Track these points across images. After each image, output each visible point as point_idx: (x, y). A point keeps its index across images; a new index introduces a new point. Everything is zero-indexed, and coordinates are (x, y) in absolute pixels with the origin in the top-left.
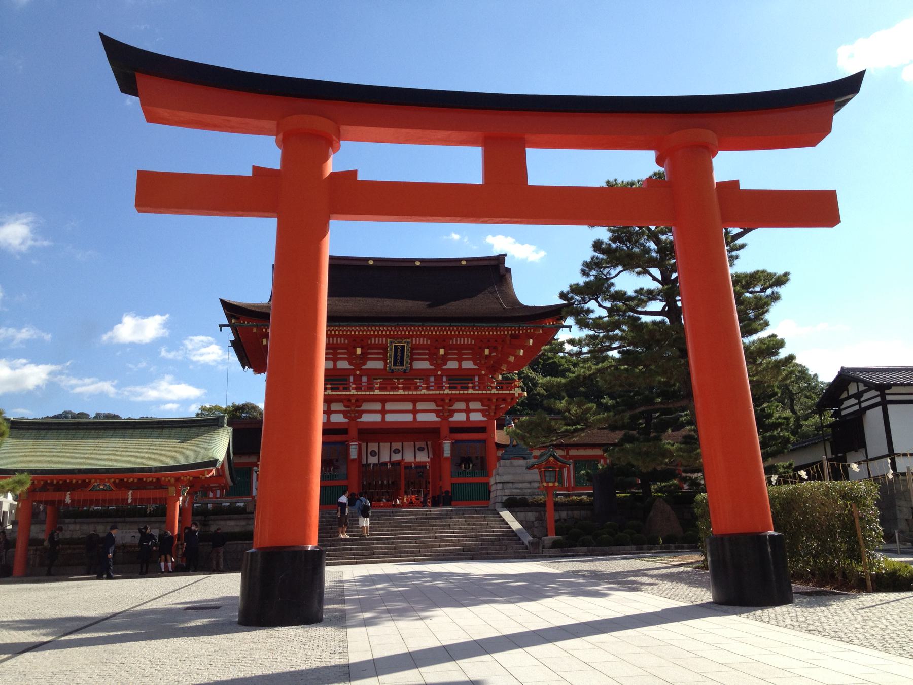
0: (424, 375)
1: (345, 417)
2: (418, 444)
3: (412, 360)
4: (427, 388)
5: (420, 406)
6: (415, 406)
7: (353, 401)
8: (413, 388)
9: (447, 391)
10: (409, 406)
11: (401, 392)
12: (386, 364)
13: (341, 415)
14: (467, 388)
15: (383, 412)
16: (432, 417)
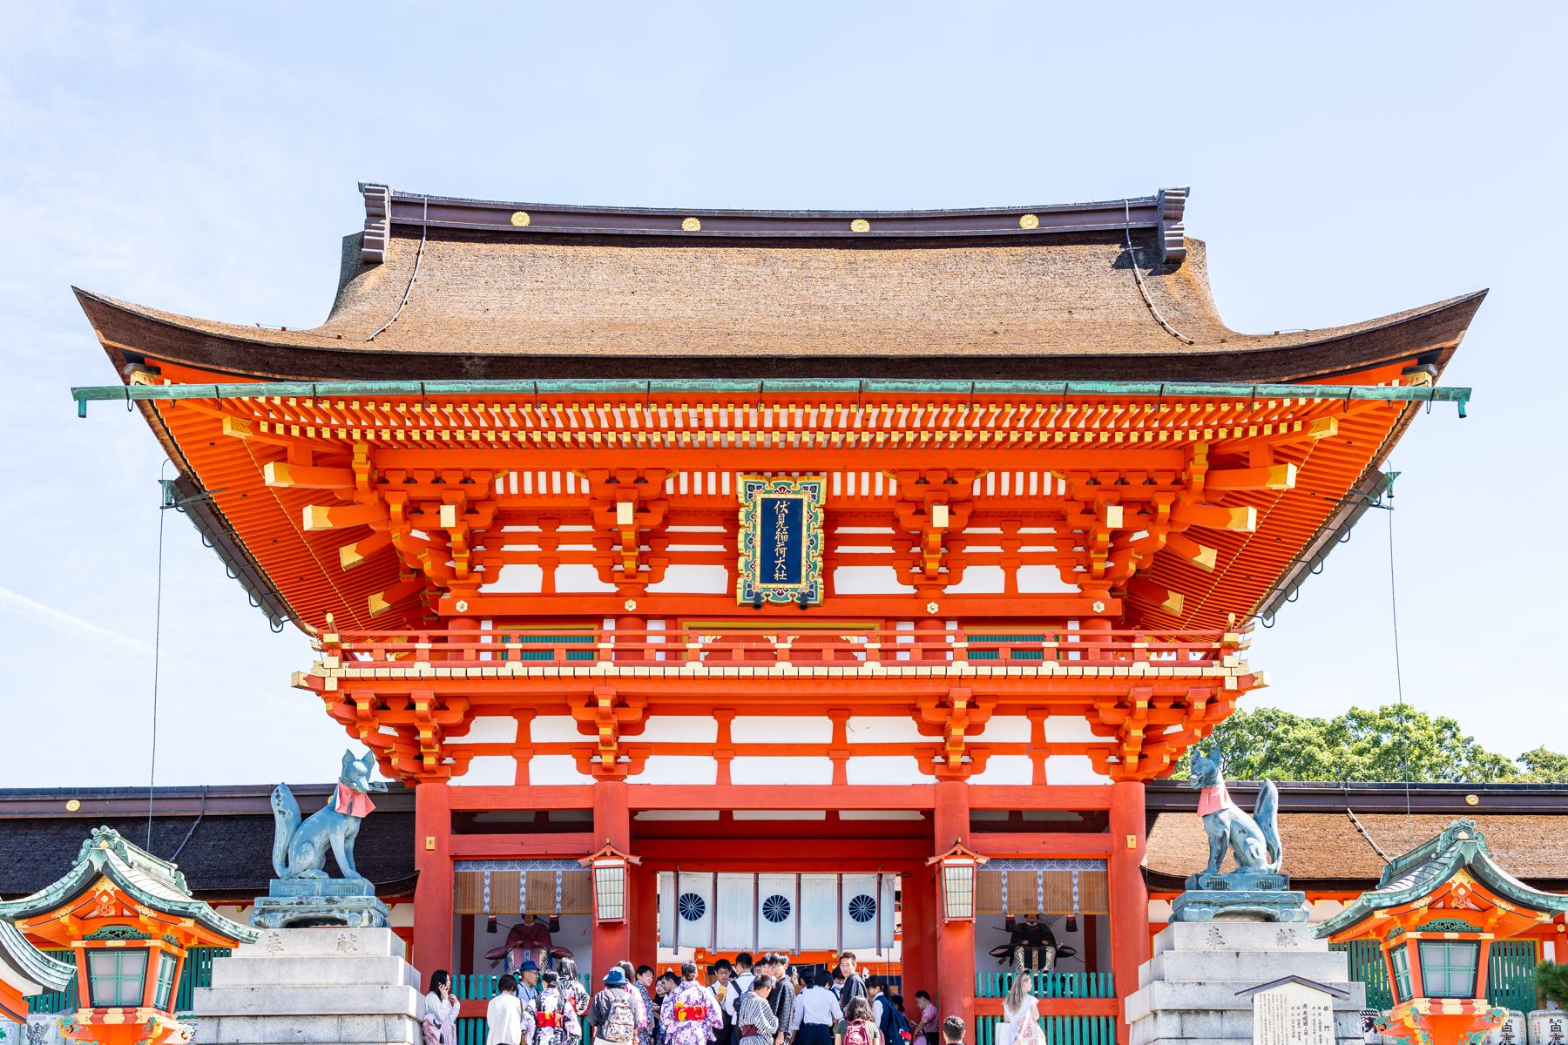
0: (881, 614)
1: (584, 767)
2: (860, 883)
3: (831, 561)
4: (887, 655)
5: (861, 729)
6: (839, 731)
7: (605, 703)
8: (828, 654)
9: (960, 668)
10: (818, 729)
11: (784, 668)
12: (734, 575)
13: (569, 761)
14: (1038, 654)
15: (724, 750)
16: (905, 773)
